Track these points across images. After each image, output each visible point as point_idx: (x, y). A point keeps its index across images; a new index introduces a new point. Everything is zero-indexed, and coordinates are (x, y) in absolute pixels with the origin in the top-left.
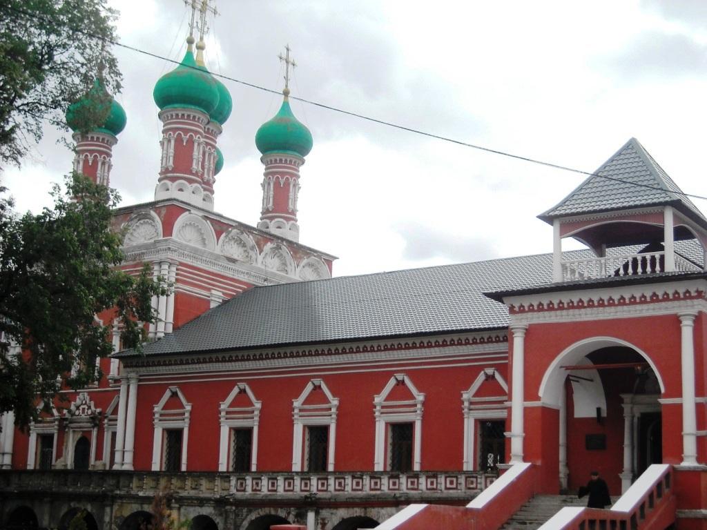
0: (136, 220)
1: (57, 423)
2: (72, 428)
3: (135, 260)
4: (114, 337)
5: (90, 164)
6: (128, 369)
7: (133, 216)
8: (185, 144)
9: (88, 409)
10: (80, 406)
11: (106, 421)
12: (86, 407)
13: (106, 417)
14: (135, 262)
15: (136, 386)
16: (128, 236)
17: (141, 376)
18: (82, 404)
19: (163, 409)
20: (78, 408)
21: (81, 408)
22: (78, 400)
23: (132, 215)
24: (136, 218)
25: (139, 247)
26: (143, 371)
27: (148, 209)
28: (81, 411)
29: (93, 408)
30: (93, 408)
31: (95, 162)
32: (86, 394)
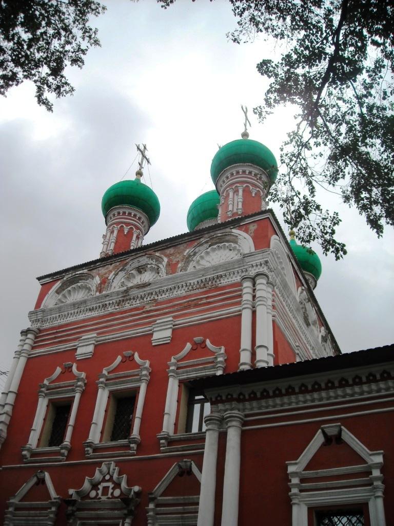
0: (206, 246)
1: (53, 509)
2: (80, 519)
3: (205, 286)
4: (171, 380)
5: (125, 233)
6: (221, 406)
7: (203, 240)
8: (253, 195)
9: (114, 489)
10: (99, 483)
11: (151, 506)
12: (111, 485)
13: (153, 500)
14: (205, 289)
15: (239, 432)
16: (191, 265)
17: (247, 416)
18: (104, 480)
19: (305, 469)
20: (95, 486)
21: (100, 487)
22: (97, 472)
23: (201, 240)
24: (206, 242)
25: (216, 268)
26: (253, 407)
27: (228, 230)
28: (100, 492)
29: (124, 485)
30: (124, 485)
31: (130, 233)
32: (113, 466)
